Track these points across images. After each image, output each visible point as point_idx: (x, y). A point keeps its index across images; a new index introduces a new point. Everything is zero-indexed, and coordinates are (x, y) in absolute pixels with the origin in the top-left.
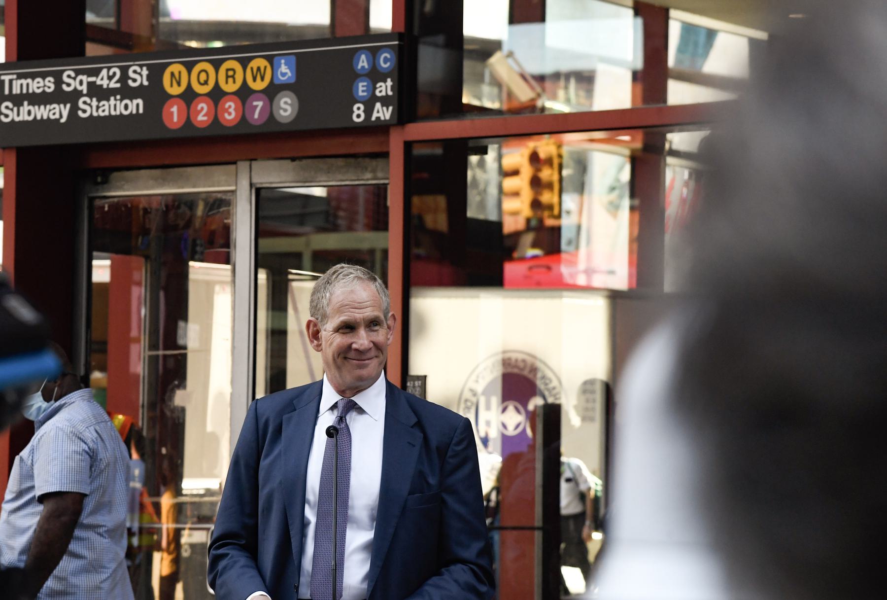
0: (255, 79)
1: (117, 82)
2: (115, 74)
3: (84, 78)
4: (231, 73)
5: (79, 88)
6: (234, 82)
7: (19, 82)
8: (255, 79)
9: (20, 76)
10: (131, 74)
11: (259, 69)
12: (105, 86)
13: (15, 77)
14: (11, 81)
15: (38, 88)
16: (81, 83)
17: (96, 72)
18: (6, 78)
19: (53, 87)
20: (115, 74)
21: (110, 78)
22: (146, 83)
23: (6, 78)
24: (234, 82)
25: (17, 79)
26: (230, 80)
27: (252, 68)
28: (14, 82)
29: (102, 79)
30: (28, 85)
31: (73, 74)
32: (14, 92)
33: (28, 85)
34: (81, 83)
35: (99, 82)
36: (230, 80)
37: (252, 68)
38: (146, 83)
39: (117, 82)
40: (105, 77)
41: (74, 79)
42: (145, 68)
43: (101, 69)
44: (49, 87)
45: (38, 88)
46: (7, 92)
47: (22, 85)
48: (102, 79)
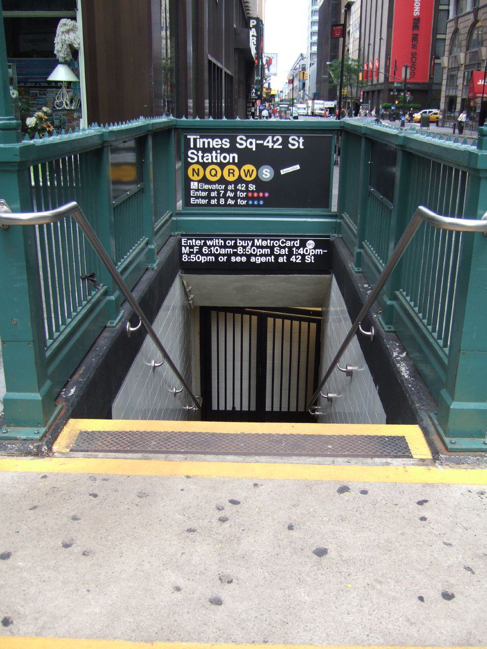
0: (246, 176)
1: (279, 145)
2: (278, 140)
3: (254, 141)
4: (231, 171)
5: (249, 146)
6: (234, 176)
7: (202, 140)
8: (246, 176)
9: (201, 137)
10: (290, 140)
11: (248, 171)
12: (270, 147)
13: (198, 137)
14: (195, 140)
15: (217, 145)
16: (251, 143)
17: (264, 138)
18: (192, 137)
19: (228, 145)
20: (278, 140)
21: (274, 142)
22: (302, 147)
23: (192, 137)
24: (234, 176)
25: (200, 138)
26: (231, 175)
27: (244, 170)
28: (198, 140)
29: (268, 142)
30: (209, 143)
31: (245, 138)
32: (198, 146)
33: (209, 143)
34: (251, 143)
35: (265, 144)
36: (231, 175)
37: (244, 170)
38: (302, 147)
39: (279, 145)
40: (271, 141)
41: (246, 141)
42: (301, 138)
43: (267, 136)
44: (226, 145)
45: (217, 145)
46: (192, 146)
47: (204, 143)
48: (268, 142)
